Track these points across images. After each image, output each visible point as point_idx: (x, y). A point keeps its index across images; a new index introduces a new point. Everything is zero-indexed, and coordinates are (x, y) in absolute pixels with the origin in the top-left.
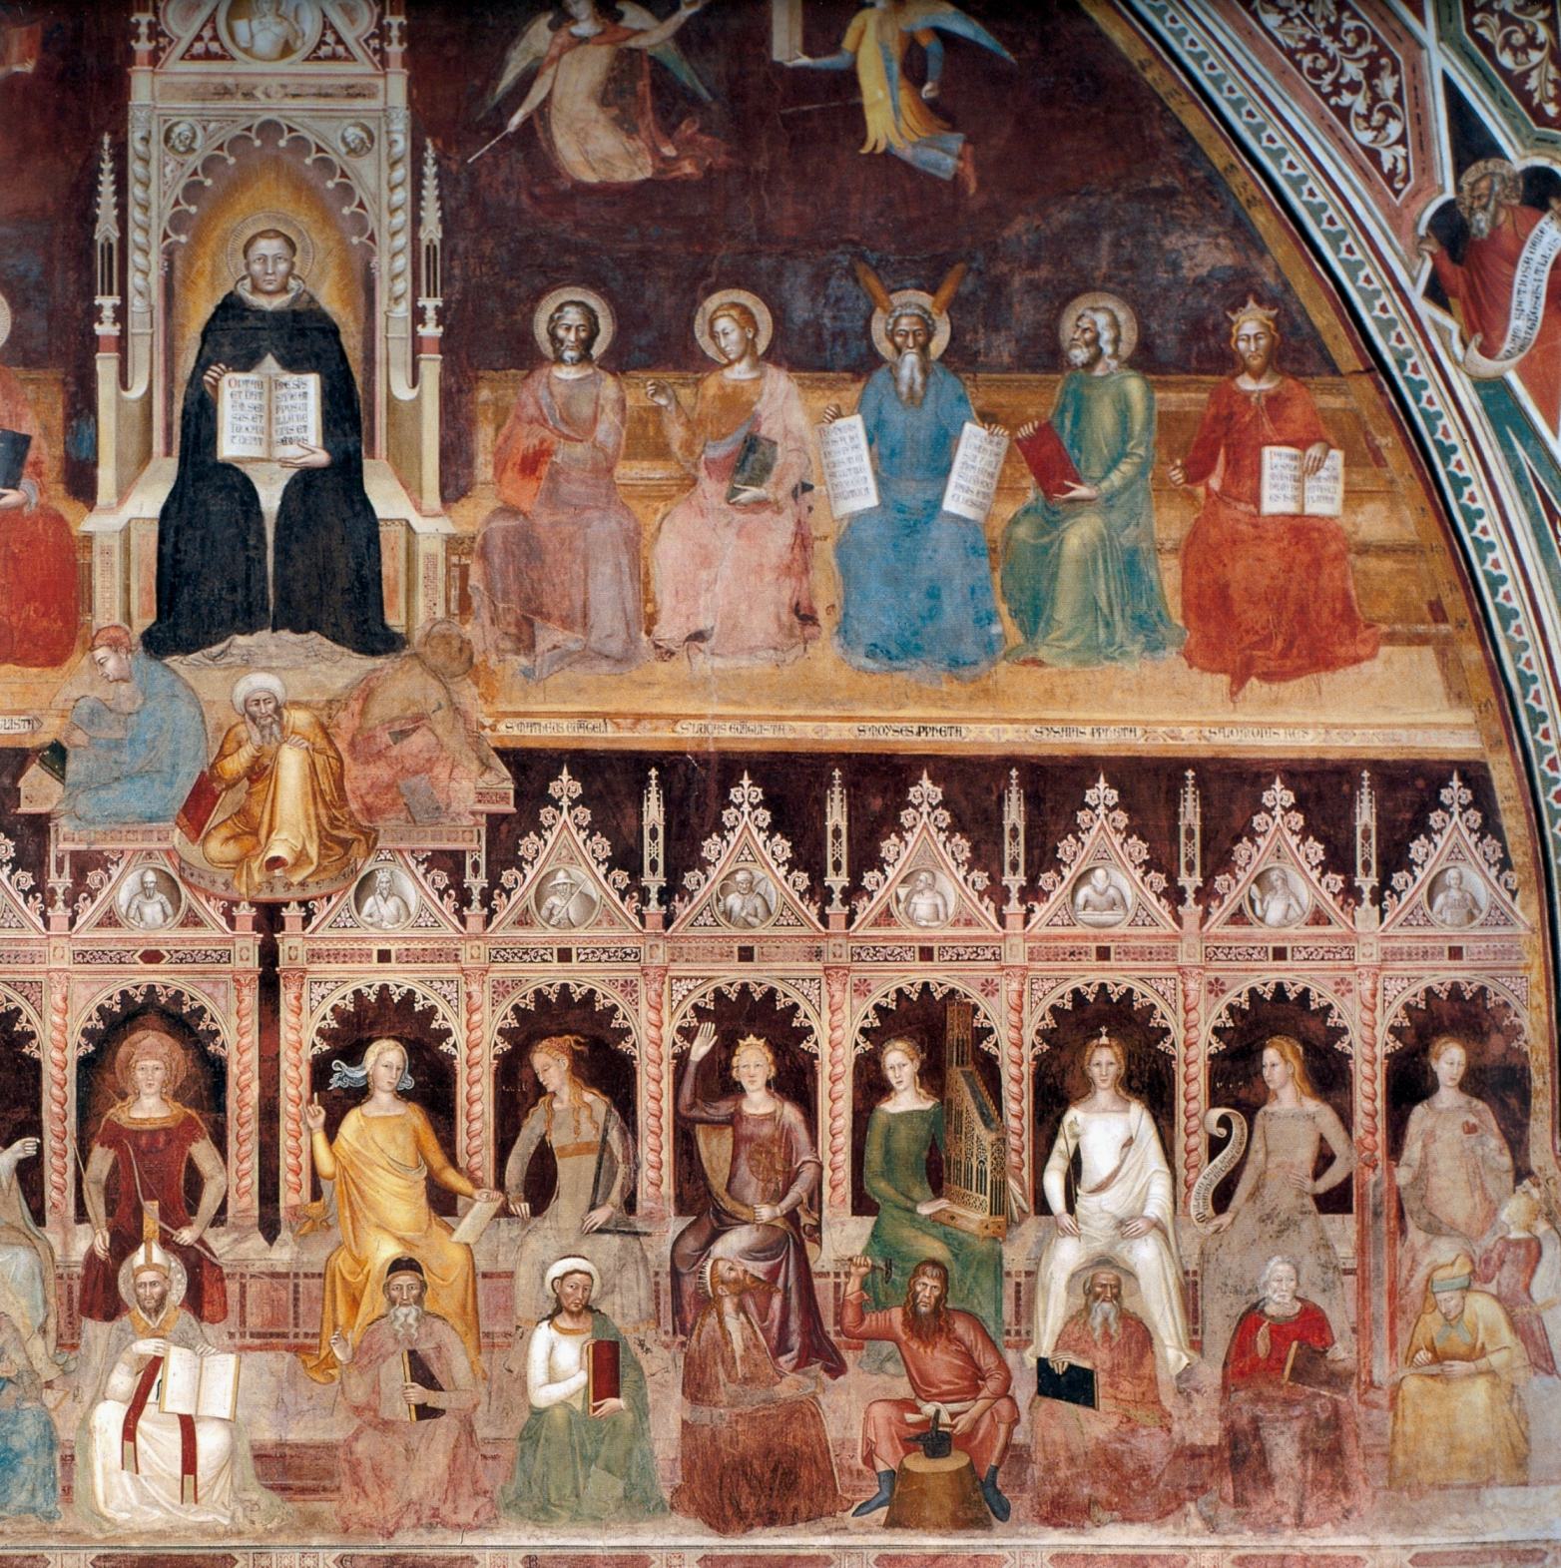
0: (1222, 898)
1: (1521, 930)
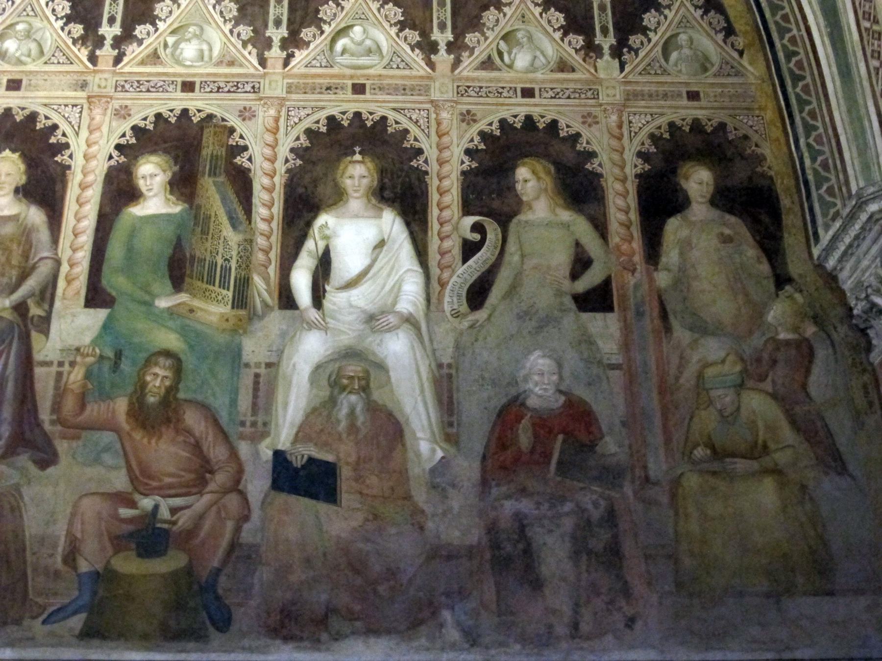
0: (472, 51)
1: (752, 80)
